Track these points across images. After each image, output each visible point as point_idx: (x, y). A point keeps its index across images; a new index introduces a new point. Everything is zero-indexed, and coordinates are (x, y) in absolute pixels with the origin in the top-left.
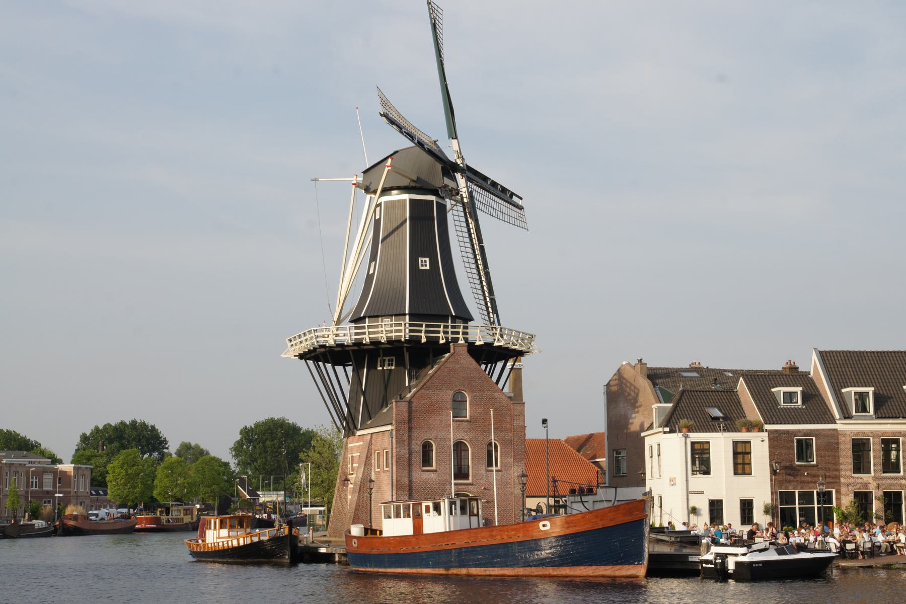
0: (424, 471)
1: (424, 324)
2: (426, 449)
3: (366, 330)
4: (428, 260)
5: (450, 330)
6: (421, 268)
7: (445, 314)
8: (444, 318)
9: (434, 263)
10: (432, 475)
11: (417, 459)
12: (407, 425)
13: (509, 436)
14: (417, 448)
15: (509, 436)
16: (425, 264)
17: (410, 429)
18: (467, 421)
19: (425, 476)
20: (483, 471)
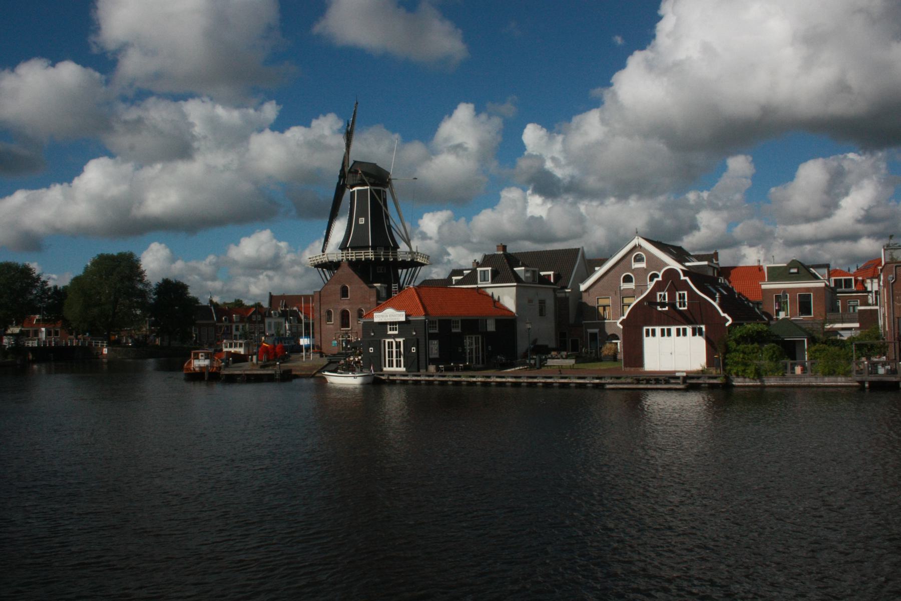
0: (328, 324)
1: (363, 252)
2: (329, 313)
3: (363, 254)
4: (364, 219)
5: (370, 254)
6: (360, 223)
7: (366, 245)
8: (367, 247)
9: (366, 221)
10: (331, 326)
11: (324, 319)
12: (319, 303)
13: (368, 306)
14: (323, 313)
15: (368, 306)
16: (362, 221)
17: (320, 304)
18: (349, 300)
19: (328, 326)
20: (356, 324)
